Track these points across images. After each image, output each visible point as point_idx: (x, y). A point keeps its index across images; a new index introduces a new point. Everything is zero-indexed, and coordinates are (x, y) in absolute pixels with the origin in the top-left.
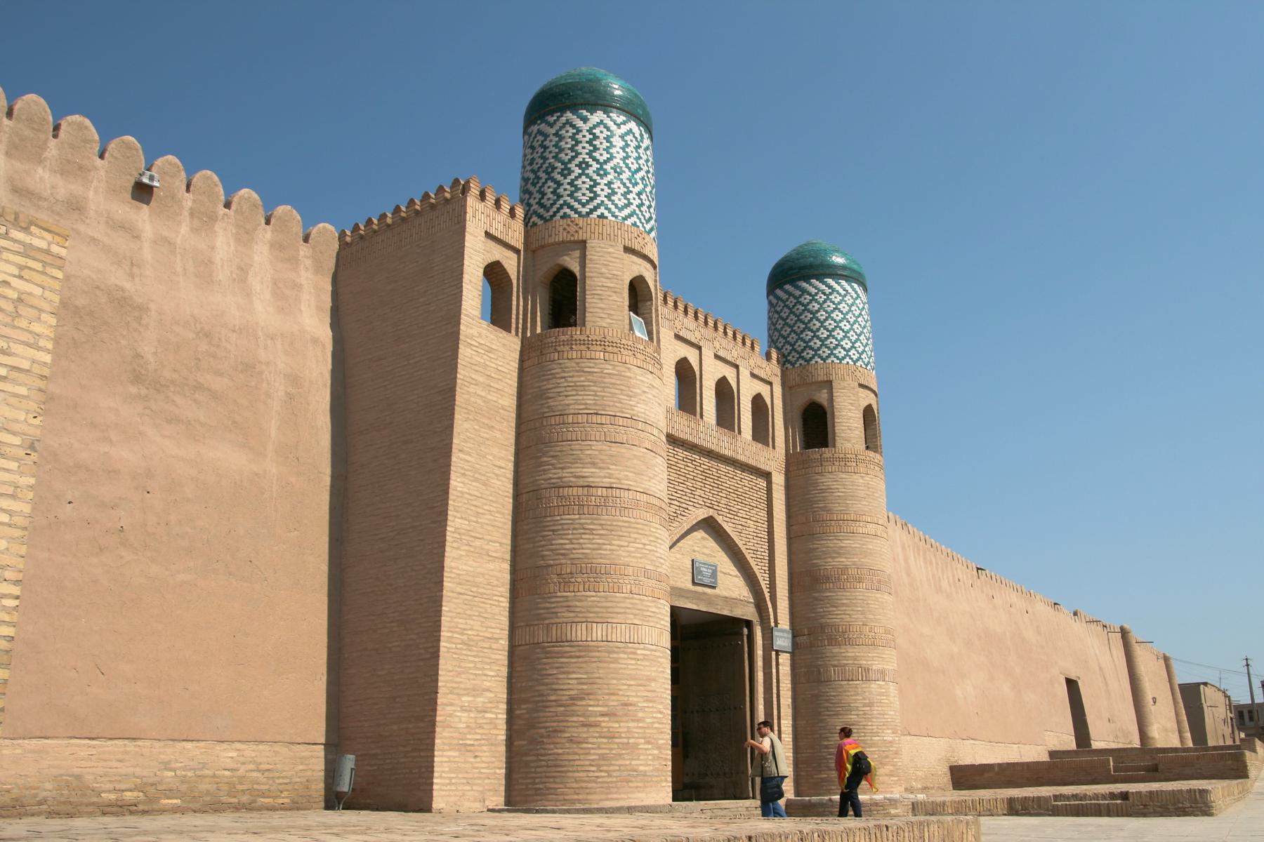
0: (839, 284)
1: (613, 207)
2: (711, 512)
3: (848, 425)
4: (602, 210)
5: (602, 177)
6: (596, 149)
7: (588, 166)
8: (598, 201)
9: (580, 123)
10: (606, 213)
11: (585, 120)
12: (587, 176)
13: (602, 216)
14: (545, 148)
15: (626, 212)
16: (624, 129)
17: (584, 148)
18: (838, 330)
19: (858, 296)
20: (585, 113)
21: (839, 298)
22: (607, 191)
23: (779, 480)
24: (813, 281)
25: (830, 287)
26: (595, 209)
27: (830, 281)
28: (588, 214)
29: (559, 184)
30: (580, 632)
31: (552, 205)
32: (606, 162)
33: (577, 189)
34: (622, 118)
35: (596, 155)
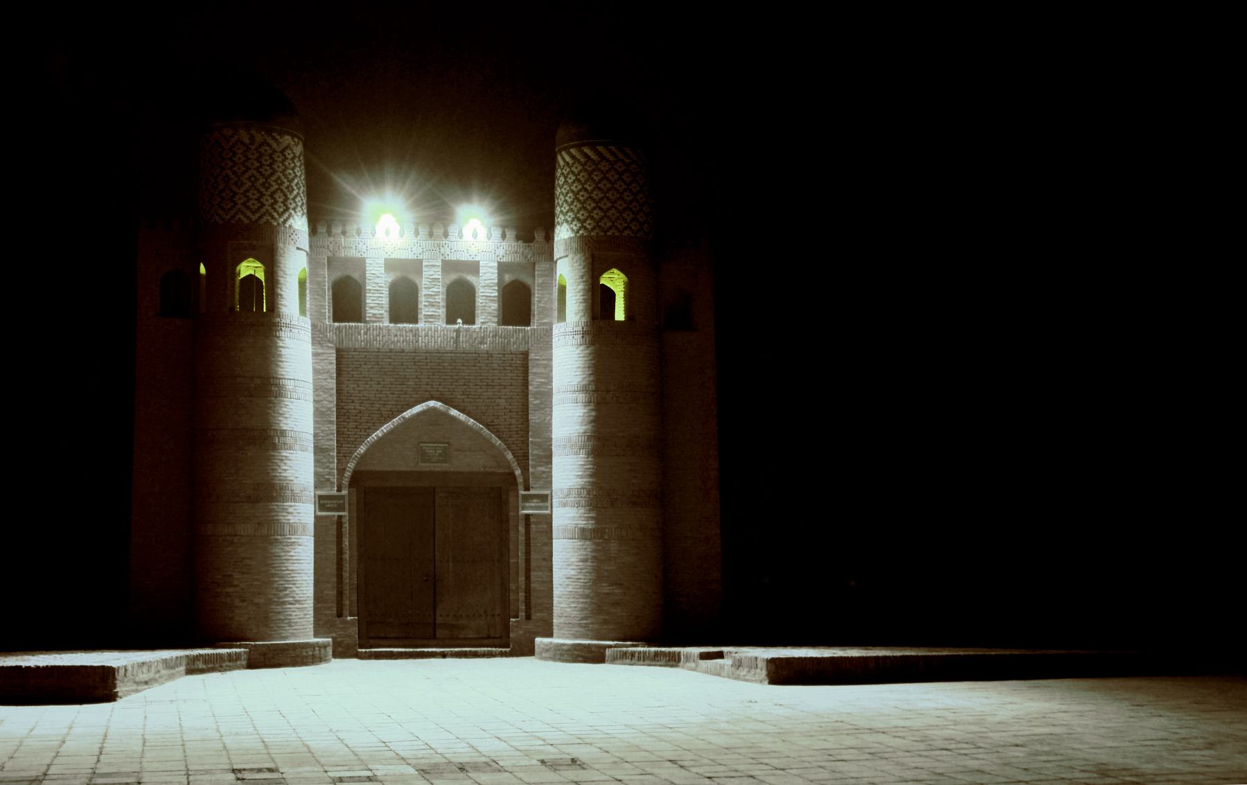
15: (232, 212)
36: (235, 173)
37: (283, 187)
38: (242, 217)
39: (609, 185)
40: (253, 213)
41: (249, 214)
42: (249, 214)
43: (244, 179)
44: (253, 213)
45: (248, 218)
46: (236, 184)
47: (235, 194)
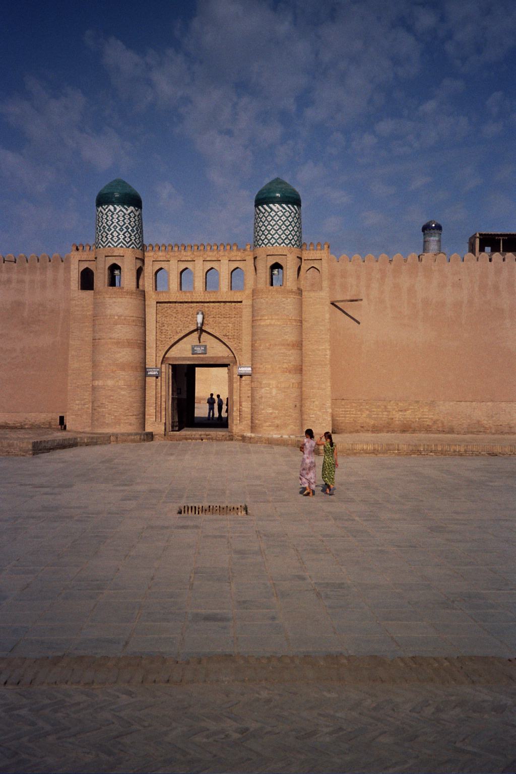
16: (107, 210)
34: (106, 206)
36: (107, 225)
38: (111, 245)
39: (275, 227)
40: (115, 242)
41: (113, 243)
42: (113, 243)
43: (111, 227)
44: (115, 242)
45: (113, 245)
46: (108, 230)
47: (108, 234)
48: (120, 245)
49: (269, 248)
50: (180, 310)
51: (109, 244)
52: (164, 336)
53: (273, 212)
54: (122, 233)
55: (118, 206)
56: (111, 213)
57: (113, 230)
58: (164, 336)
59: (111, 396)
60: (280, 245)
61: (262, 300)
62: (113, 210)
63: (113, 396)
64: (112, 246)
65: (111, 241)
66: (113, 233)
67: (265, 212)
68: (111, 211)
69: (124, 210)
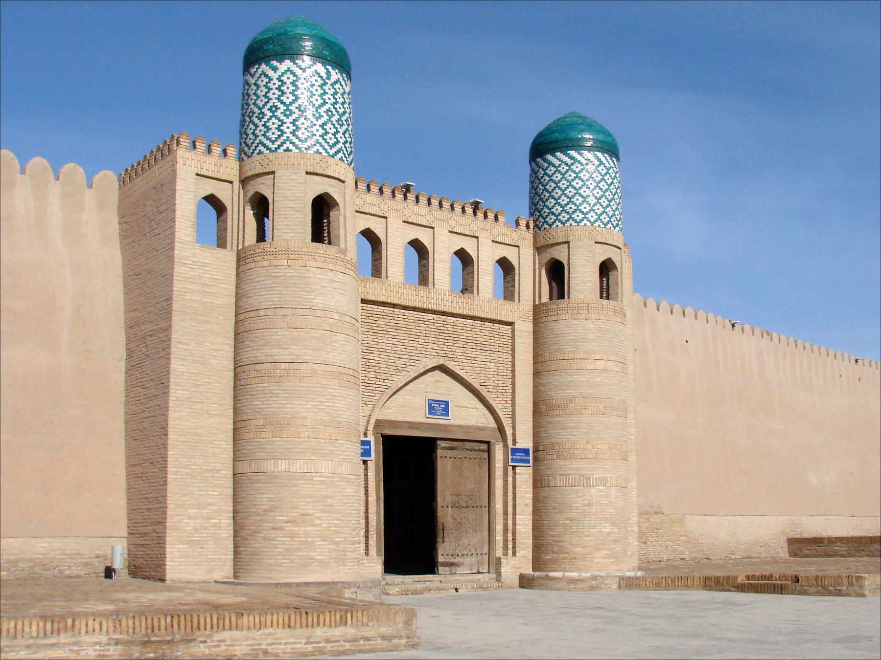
0: (581, 155)
1: (297, 141)
2: (441, 361)
3: (583, 278)
4: (288, 144)
5: (287, 116)
6: (283, 93)
7: (277, 108)
8: (284, 138)
9: (271, 73)
10: (291, 147)
11: (275, 69)
12: (276, 117)
13: (288, 150)
14: (270, 89)
17: (274, 94)
18: (577, 197)
19: (601, 163)
20: (275, 63)
21: (580, 167)
22: (292, 128)
23: (525, 328)
24: (558, 154)
25: (572, 158)
26: (282, 144)
27: (572, 153)
28: (276, 149)
29: (256, 126)
30: (269, 466)
31: (253, 143)
32: (291, 103)
33: (269, 129)
35: (284, 98)
37: (278, 113)
38: (321, 150)
41: (326, 147)
45: (326, 150)
48: (340, 155)
49: (599, 229)
50: (403, 324)
51: (318, 147)
52: (372, 375)
53: (602, 167)
54: (342, 131)
55: (333, 69)
56: (321, 82)
57: (326, 118)
58: (372, 375)
59: (325, 497)
60: (615, 228)
61: (586, 322)
62: (325, 76)
63: (330, 497)
64: (324, 154)
65: (321, 140)
66: (324, 124)
67: (560, 165)
68: (321, 77)
69: (343, 83)
